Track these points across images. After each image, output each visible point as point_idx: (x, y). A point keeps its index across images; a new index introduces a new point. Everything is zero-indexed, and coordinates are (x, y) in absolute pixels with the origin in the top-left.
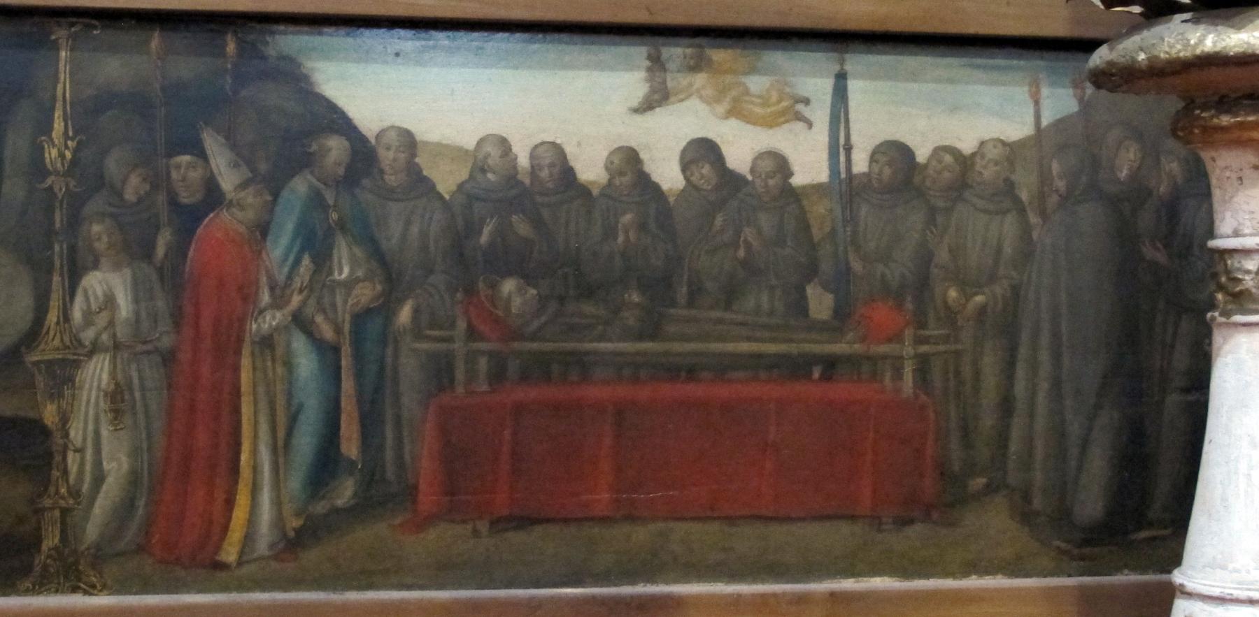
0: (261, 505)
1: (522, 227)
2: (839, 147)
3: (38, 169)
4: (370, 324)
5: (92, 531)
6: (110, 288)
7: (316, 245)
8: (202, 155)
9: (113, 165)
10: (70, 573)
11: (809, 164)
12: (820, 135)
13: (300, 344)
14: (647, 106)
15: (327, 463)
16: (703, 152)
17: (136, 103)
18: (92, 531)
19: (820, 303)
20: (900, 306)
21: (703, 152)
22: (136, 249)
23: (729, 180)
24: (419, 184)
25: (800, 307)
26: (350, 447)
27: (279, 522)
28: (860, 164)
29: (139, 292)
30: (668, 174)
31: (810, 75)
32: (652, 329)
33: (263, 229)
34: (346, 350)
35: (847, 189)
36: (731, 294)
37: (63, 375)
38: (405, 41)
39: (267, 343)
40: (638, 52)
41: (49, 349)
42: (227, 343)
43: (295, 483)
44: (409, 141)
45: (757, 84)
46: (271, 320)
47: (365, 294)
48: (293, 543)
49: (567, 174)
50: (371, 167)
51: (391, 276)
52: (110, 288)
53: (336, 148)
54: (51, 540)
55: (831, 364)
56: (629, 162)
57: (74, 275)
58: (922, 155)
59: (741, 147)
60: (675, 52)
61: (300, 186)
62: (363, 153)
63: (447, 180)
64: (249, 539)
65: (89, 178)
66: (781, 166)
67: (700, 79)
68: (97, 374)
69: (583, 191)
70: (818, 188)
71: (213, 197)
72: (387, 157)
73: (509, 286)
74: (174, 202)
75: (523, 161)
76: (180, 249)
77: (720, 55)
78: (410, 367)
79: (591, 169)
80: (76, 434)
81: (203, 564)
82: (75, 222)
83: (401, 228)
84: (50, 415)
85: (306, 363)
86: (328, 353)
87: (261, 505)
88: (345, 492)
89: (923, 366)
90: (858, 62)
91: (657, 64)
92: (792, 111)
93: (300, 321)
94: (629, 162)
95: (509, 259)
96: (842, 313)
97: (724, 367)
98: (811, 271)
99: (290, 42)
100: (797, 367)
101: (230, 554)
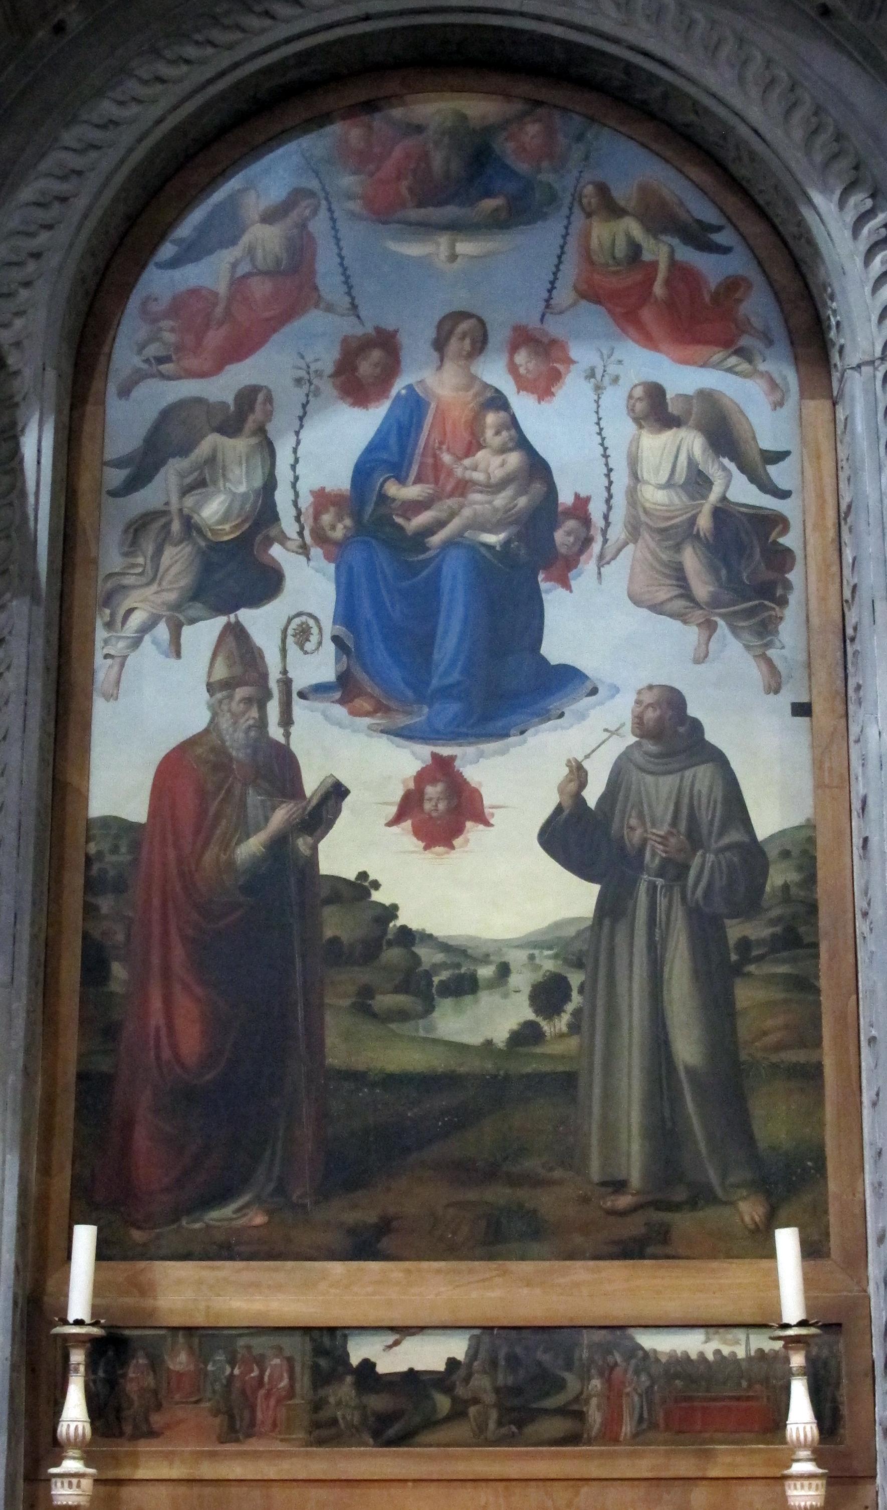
0: (627, 1428)
1: (679, 1368)
2: (748, 1349)
3: (581, 1359)
4: (649, 1390)
5: (593, 1433)
6: (596, 1384)
7: (637, 1373)
8: (613, 1355)
9: (596, 1357)
10: (589, 1443)
11: (741, 1353)
12: (743, 1347)
13: (634, 1393)
14: (706, 1342)
15: (641, 1419)
16: (718, 1352)
17: (599, 1345)
18: (593, 1433)
19: (744, 1384)
20: (762, 1385)
21: (718, 1352)
22: (601, 1374)
23: (724, 1358)
24: (657, 1360)
25: (739, 1384)
26: (646, 1415)
27: (631, 1432)
28: (753, 1353)
29: (602, 1384)
30: (710, 1357)
31: (741, 1334)
32: (708, 1391)
33: (626, 1371)
34: (644, 1396)
35: (749, 1359)
36: (724, 1383)
37: (587, 1402)
38: (654, 1330)
39: (628, 1394)
40: (702, 1330)
41: (584, 1396)
42: (620, 1396)
43: (634, 1423)
44: (655, 1351)
45: (730, 1337)
46: (628, 1390)
47: (648, 1383)
48: (635, 1435)
49: (688, 1357)
50: (647, 1357)
51: (653, 1380)
52: (596, 1384)
53: (640, 1353)
54: (585, 1436)
55: (748, 1398)
56: (702, 1355)
57: (589, 1380)
58: (767, 1351)
59: (726, 1351)
60: (711, 1330)
61: (633, 1361)
62: (646, 1354)
63: (664, 1360)
64: (626, 1434)
65: (591, 1360)
66: (734, 1354)
67: (716, 1336)
68: (594, 1401)
69: (692, 1360)
70: (743, 1360)
71: (616, 1364)
72: (651, 1355)
73: (677, 1382)
74: (608, 1365)
75: (679, 1355)
76: (611, 1373)
77: (721, 1330)
78: (657, 1398)
79: (694, 1356)
80: (590, 1412)
81: (616, 1441)
82: (589, 1371)
83: (654, 1370)
84: (585, 1409)
85: (636, 1398)
86: (640, 1396)
87: (627, 1428)
88: (644, 1426)
89: (768, 1398)
90: (751, 1331)
91: (707, 1333)
92: (737, 1342)
93: (635, 1390)
94: (702, 1355)
95: (677, 1376)
96: (750, 1386)
97: (723, 1399)
98: (742, 1377)
99: (631, 1331)
100: (738, 1399)
101: (622, 1438)
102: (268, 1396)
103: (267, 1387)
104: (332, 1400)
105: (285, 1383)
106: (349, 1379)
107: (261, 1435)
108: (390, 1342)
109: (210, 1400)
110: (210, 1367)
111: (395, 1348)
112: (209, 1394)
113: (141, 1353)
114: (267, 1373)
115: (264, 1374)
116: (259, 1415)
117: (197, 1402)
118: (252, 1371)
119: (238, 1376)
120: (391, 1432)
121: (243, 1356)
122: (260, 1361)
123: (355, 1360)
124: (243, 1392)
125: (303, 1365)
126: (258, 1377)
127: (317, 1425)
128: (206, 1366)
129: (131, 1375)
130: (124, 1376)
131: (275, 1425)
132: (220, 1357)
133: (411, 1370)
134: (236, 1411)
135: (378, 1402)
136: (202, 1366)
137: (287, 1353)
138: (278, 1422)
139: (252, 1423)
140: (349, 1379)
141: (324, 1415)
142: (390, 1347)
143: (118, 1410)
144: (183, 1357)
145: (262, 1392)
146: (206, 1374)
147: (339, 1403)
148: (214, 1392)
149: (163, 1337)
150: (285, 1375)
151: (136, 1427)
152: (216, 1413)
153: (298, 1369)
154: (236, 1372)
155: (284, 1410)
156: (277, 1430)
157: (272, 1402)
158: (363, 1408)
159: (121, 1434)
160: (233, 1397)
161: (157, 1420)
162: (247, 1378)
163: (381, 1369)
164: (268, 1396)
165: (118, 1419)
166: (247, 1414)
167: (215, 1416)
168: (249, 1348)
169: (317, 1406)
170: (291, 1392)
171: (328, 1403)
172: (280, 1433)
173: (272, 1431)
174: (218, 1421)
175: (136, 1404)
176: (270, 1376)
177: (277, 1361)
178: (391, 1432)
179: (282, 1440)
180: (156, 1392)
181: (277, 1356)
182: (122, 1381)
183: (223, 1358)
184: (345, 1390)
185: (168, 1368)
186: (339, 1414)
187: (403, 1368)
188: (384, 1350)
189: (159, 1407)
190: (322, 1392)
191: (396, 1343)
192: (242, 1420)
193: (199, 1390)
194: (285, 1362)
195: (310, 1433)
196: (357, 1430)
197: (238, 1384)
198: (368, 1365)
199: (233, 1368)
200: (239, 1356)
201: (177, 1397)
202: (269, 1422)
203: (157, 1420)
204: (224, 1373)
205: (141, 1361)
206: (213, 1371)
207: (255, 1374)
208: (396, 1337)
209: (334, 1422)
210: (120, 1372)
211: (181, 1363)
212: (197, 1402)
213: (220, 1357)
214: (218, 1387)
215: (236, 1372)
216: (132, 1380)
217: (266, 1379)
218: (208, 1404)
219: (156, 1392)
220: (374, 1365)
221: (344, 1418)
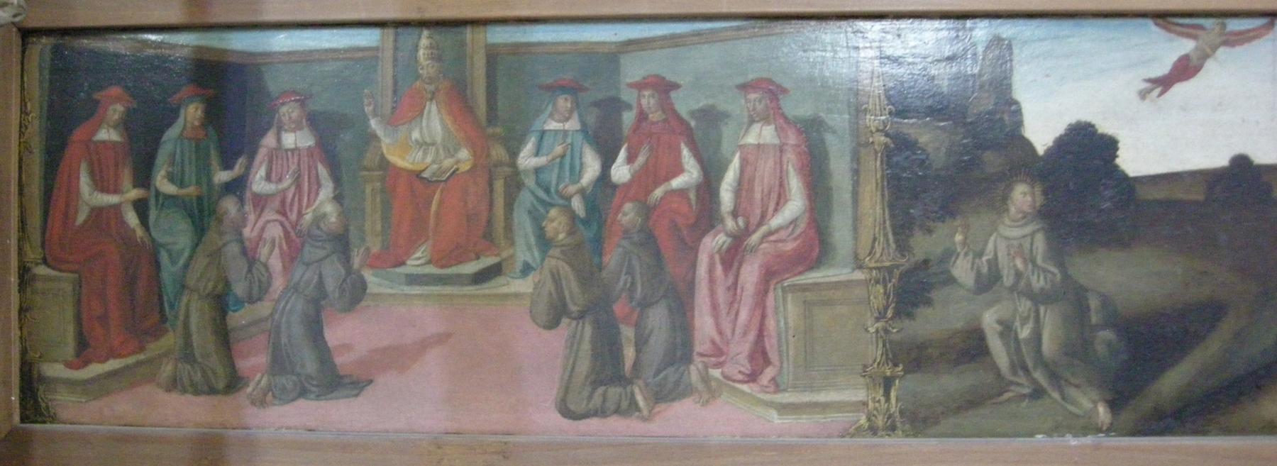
102: (732, 257)
103: (730, 223)
104: (962, 270)
105: (795, 205)
106: (1023, 196)
107: (711, 391)
108: (1162, 68)
109: (527, 269)
110: (527, 159)
111: (1179, 89)
112: (524, 251)
113: (289, 111)
114: (730, 176)
115: (720, 179)
116: (704, 324)
117: (481, 277)
118: (678, 170)
119: (627, 186)
120: (1173, 381)
121: (642, 116)
122: (703, 134)
123: (1042, 132)
124: (648, 240)
125: (859, 147)
126: (699, 188)
127: (913, 357)
128: (514, 154)
129: (259, 184)
130: (237, 187)
131: (760, 356)
132: (560, 121)
133: (1241, 162)
134: (619, 308)
135: (1130, 278)
136: (498, 152)
137: (798, 107)
138: (771, 345)
139: (681, 351)
140: (1023, 196)
141: (938, 319)
142: (1164, 83)
143: (221, 303)
144: (436, 120)
145: (715, 242)
146: (515, 183)
147: (988, 282)
148: (544, 242)
149: (367, 57)
150: (795, 184)
151: (280, 363)
152: (556, 314)
153: (839, 167)
154: (621, 172)
155: (792, 310)
156: (769, 372)
157: (750, 274)
158: (1073, 297)
159: (234, 383)
160: (612, 259)
161: (348, 335)
162: (658, 192)
163: (1132, 162)
164: (732, 257)
165: (224, 337)
166: (658, 318)
167: (553, 324)
168: (664, 88)
169: (912, 288)
170: (816, 247)
171: (951, 280)
172: (777, 386)
173: (752, 377)
174: (557, 339)
175: (278, 284)
176: (742, 188)
177: (763, 134)
178: (1173, 381)
179: (784, 409)
180: (342, 243)
181: (766, 120)
182: (229, 205)
183: (573, 125)
184: (1010, 234)
185: (384, 164)
186: (989, 320)
187: (1218, 159)
188: (1143, 95)
189: (355, 294)
190: (923, 245)
191: (1185, 70)
192: (641, 343)
193: (488, 235)
194: (792, 139)
195: (888, 384)
196: (1054, 377)
197: (628, 214)
198: (1088, 149)
199: (608, 161)
200: (628, 118)
201: (417, 262)
202: (741, 349)
203: (348, 335)
204: (576, 173)
205: (289, 140)
206: (537, 171)
207: (689, 175)
208: (1186, 46)
209: (971, 348)
210: (222, 176)
211: (423, 145)
212: (481, 277)
213: (560, 121)
214: (556, 223)
215: (621, 172)
216: (261, 202)
217: (726, 196)
218: (523, 286)
219: (342, 243)
220: (1109, 145)
221: (1007, 330)
